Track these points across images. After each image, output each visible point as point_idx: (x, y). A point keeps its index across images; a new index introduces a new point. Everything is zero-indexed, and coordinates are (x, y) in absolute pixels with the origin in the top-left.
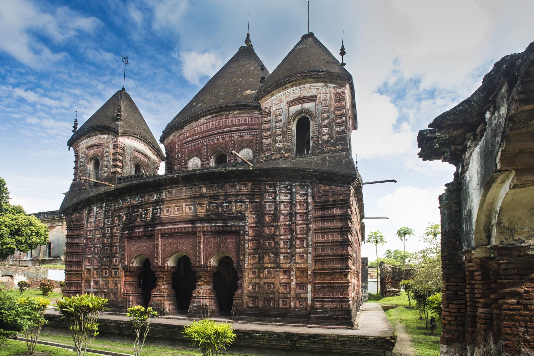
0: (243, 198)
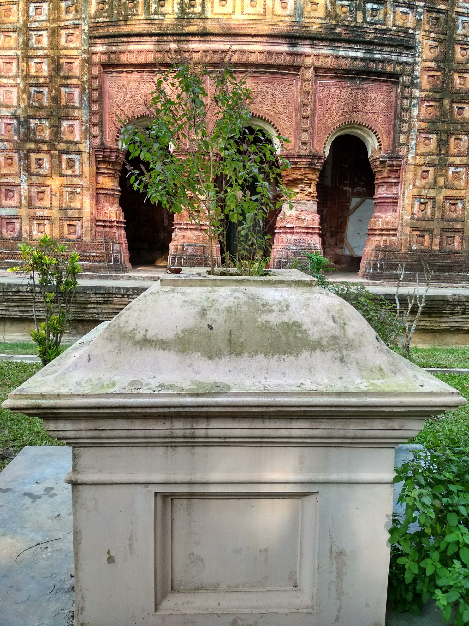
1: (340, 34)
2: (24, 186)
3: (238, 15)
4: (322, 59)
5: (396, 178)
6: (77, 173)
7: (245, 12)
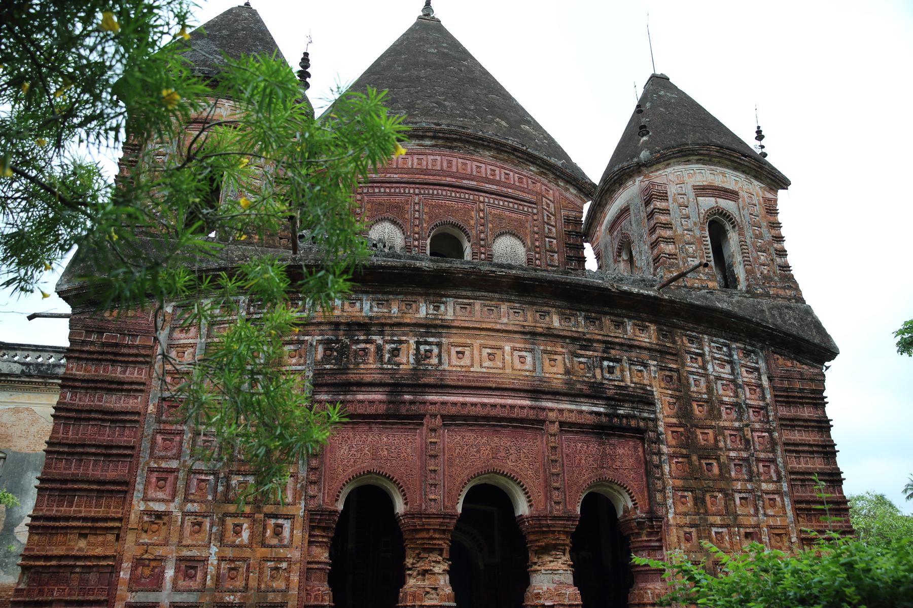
0: (642, 356)
1: (581, 390)
2: (213, 560)
3: (476, 368)
4: (566, 414)
5: (657, 541)
6: (286, 542)
7: (484, 365)
